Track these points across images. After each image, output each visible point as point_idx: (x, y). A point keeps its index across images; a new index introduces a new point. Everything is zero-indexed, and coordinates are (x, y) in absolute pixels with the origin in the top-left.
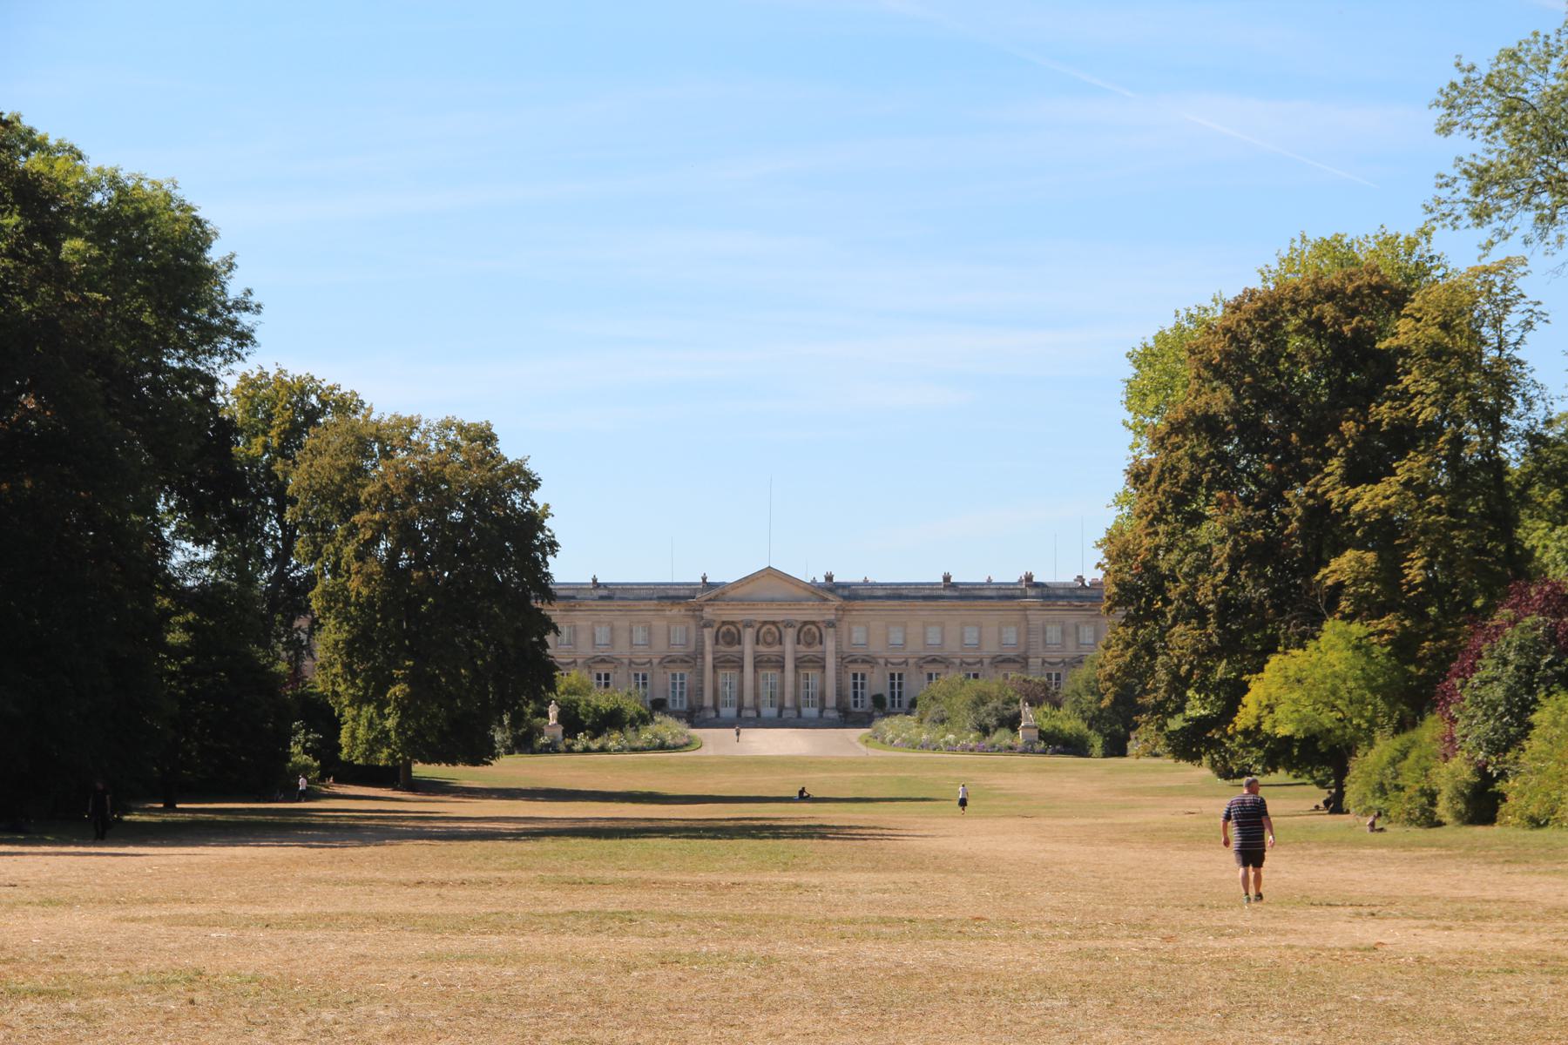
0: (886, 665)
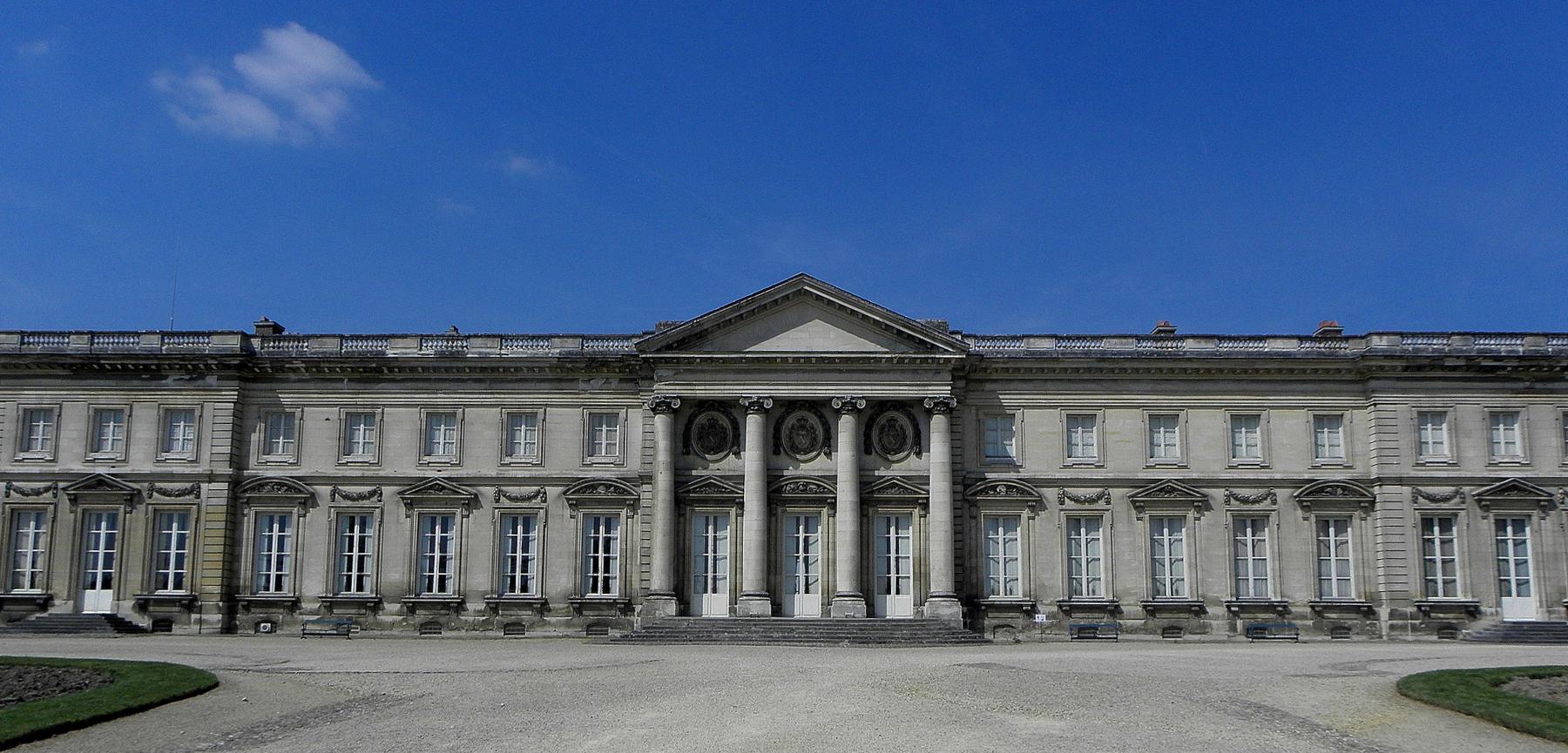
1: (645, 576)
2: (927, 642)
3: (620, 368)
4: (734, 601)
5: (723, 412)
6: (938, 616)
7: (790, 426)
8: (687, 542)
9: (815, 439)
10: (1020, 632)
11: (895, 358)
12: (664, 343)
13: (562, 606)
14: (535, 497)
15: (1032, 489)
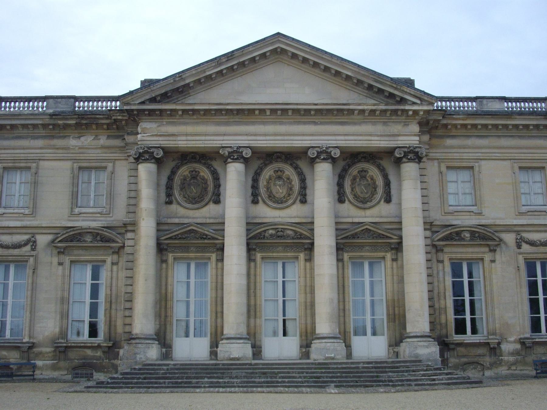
0: (519, 246)
1: (128, 321)
2: (416, 385)
3: (108, 125)
4: (214, 344)
5: (204, 164)
6: (417, 356)
7: (267, 177)
8: (169, 288)
9: (291, 189)
10: (488, 368)
11: (367, 110)
12: (148, 97)
13: (48, 350)
14: (26, 244)
15: (493, 234)
